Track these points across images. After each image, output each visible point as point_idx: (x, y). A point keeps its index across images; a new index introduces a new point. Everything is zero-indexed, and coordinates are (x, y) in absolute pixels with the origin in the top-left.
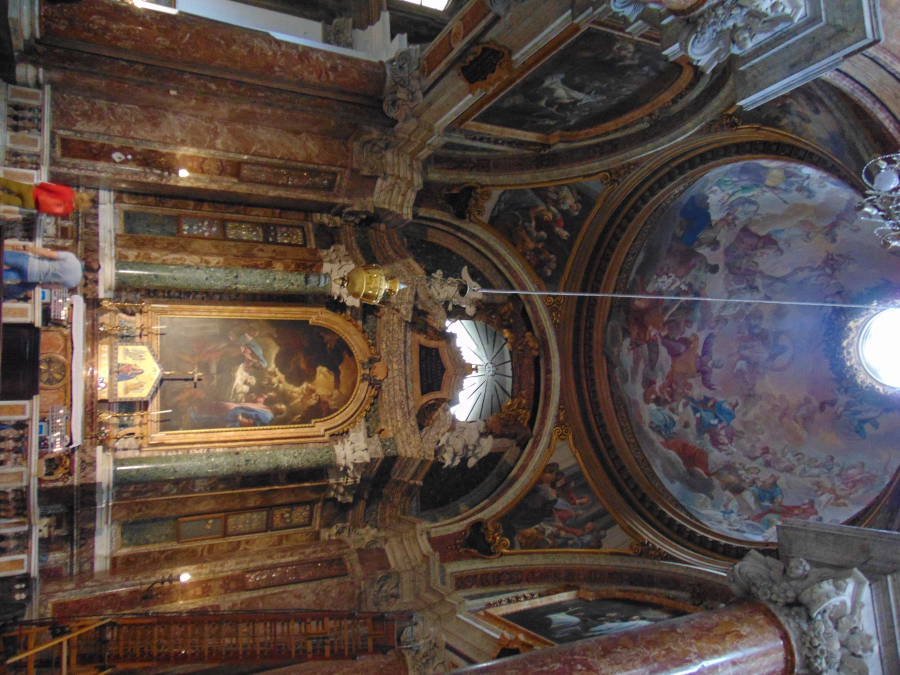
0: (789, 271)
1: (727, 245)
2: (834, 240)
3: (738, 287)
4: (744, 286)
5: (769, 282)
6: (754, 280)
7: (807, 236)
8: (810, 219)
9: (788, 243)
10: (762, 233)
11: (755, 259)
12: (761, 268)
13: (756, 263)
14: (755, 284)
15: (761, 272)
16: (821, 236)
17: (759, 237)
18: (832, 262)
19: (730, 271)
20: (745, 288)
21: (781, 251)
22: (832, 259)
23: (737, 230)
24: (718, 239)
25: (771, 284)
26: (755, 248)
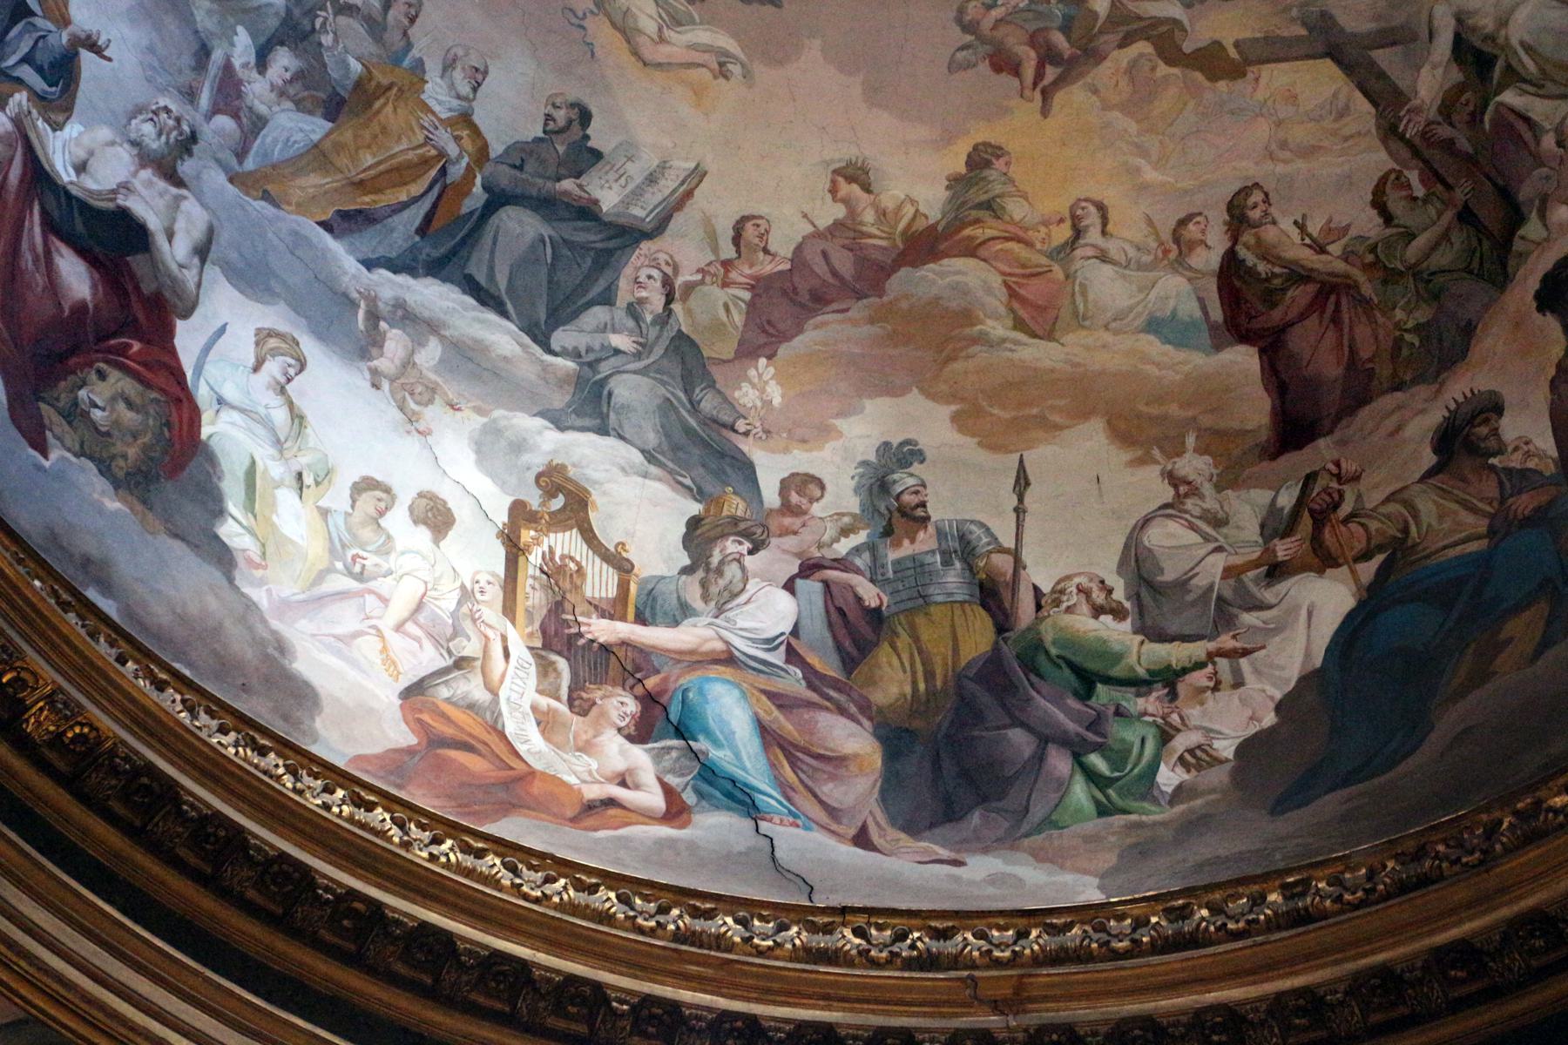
0: (1275, 77)
1: (1423, 391)
2: (981, 159)
3: (1538, 108)
4: (1509, 97)
5: (1382, 57)
6: (1447, 109)
7: (1078, 233)
8: (997, 329)
9: (1181, 242)
10: (1244, 360)
11: (1367, 223)
12: (1378, 160)
13: (1379, 204)
14: (1456, 75)
15: (1390, 132)
16: (1016, 209)
17: (1272, 346)
18: (1059, 39)
19: (1516, 218)
20: (1513, 76)
21: (1238, 217)
22: (1048, 56)
23: (1323, 450)
24: (1429, 459)
25: (1389, 37)
26: (1329, 291)
